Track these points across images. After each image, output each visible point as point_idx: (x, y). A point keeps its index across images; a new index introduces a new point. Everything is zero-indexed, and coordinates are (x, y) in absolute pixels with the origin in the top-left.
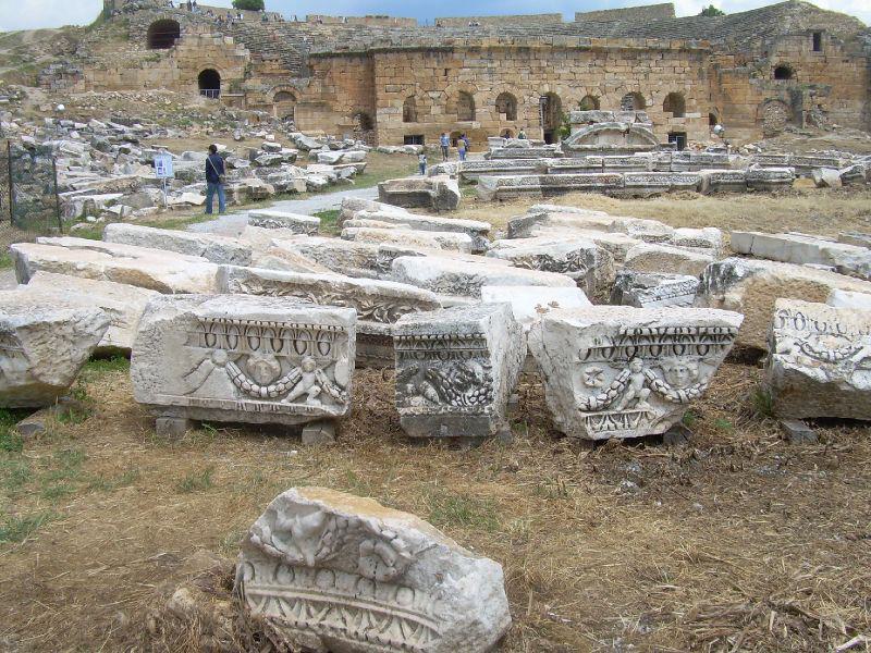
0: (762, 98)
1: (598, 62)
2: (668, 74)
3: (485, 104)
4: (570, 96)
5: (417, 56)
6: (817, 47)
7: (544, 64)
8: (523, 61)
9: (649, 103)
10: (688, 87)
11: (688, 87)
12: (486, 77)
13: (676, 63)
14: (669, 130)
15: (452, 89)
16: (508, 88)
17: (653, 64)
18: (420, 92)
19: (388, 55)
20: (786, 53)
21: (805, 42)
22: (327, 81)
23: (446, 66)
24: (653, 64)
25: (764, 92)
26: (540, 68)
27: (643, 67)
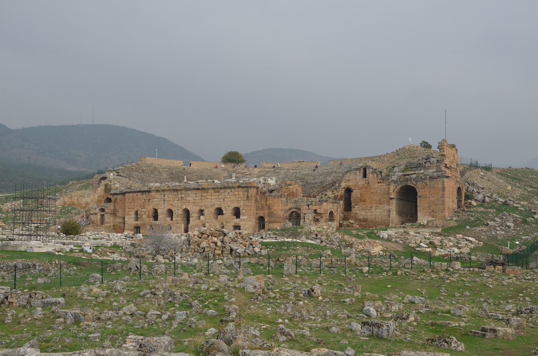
0: (287, 208)
1: (205, 194)
2: (233, 198)
3: (162, 214)
4: (194, 210)
5: (139, 194)
6: (365, 176)
7: (183, 196)
8: (176, 195)
9: (224, 212)
10: (242, 204)
11: (242, 204)
12: (162, 202)
13: (237, 193)
14: (233, 224)
15: (151, 208)
16: (170, 207)
17: (226, 194)
18: (140, 209)
19: (130, 194)
20: (349, 181)
21: (358, 174)
22: (116, 204)
23: (149, 198)
24: (226, 194)
25: (288, 204)
26: (182, 198)
27: (222, 196)
